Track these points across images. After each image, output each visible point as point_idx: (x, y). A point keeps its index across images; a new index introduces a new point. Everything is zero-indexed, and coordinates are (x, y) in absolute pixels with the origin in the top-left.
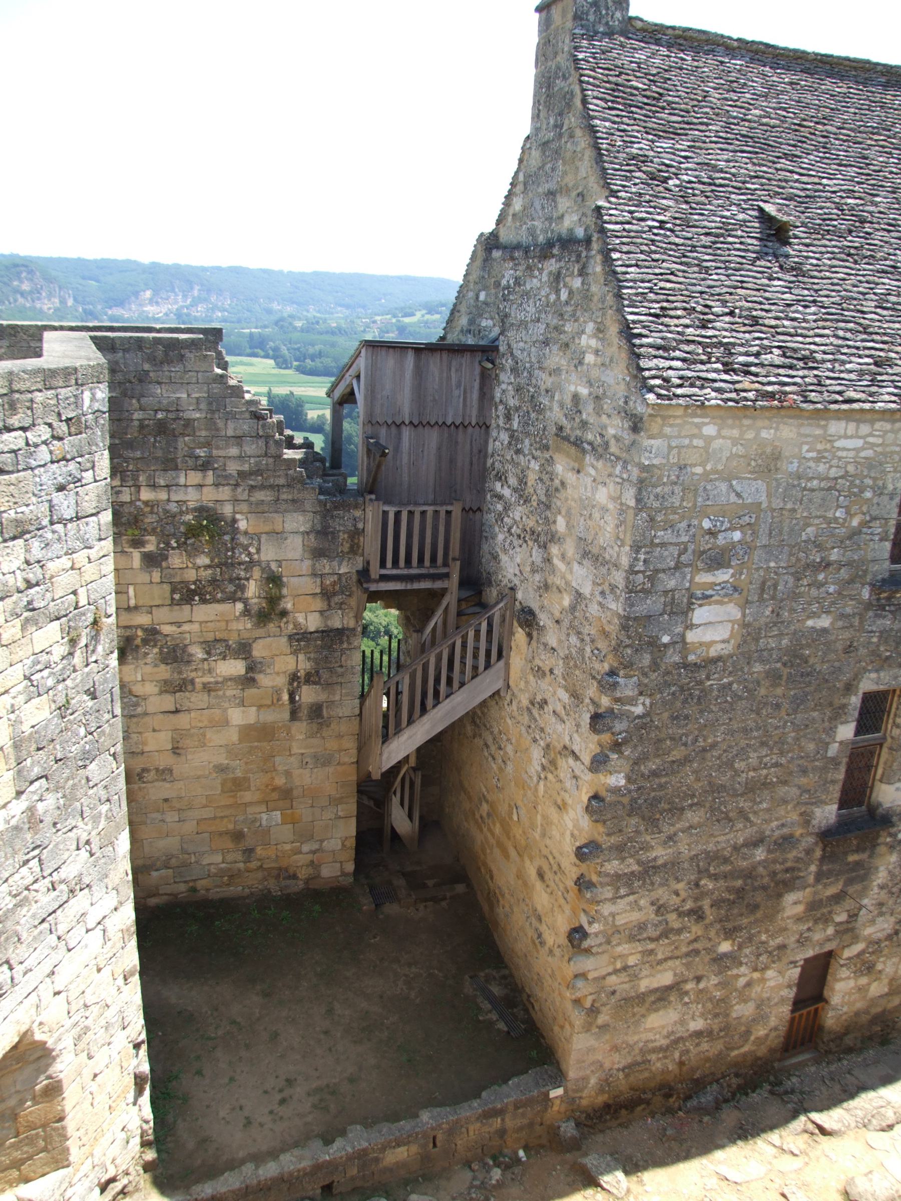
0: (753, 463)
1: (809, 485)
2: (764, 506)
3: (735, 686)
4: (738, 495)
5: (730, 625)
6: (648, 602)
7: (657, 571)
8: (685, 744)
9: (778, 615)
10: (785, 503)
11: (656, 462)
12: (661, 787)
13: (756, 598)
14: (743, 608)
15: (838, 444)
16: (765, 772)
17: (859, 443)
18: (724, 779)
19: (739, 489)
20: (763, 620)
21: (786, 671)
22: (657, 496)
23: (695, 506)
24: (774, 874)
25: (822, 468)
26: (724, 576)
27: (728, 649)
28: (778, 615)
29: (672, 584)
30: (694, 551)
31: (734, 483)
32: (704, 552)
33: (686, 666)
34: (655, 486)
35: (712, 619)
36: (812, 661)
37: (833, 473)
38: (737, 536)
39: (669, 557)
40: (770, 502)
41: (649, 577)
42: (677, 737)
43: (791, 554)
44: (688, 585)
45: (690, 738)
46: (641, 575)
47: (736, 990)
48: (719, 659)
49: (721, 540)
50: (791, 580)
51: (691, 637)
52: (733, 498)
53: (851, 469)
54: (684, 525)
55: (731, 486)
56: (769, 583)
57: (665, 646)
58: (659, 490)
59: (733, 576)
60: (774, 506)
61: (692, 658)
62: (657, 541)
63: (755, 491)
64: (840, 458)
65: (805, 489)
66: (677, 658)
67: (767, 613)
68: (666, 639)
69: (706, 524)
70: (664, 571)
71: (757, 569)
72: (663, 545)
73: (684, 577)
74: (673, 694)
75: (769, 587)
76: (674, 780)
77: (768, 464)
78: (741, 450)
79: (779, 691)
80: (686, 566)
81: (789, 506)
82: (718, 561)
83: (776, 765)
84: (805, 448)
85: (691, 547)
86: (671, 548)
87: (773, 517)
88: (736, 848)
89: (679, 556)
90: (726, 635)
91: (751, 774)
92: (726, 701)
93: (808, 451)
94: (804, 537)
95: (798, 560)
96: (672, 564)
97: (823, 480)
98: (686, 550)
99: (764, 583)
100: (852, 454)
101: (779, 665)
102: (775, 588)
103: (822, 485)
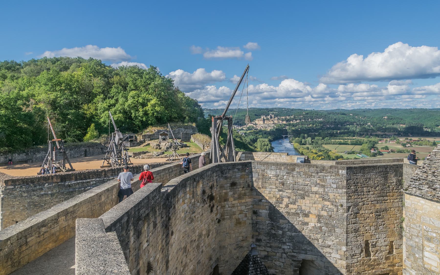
22: (410, 214)
23: (421, 220)
26: (433, 246)
29: (417, 240)
30: (422, 234)
32: (425, 235)
33: (425, 268)
35: (430, 257)
38: (434, 235)
39: (415, 232)
51: (425, 259)
54: (418, 225)
61: (426, 266)
72: (413, 228)
73: (420, 240)
78: (432, 210)
85: (421, 232)
90: (436, 265)
96: (416, 235)
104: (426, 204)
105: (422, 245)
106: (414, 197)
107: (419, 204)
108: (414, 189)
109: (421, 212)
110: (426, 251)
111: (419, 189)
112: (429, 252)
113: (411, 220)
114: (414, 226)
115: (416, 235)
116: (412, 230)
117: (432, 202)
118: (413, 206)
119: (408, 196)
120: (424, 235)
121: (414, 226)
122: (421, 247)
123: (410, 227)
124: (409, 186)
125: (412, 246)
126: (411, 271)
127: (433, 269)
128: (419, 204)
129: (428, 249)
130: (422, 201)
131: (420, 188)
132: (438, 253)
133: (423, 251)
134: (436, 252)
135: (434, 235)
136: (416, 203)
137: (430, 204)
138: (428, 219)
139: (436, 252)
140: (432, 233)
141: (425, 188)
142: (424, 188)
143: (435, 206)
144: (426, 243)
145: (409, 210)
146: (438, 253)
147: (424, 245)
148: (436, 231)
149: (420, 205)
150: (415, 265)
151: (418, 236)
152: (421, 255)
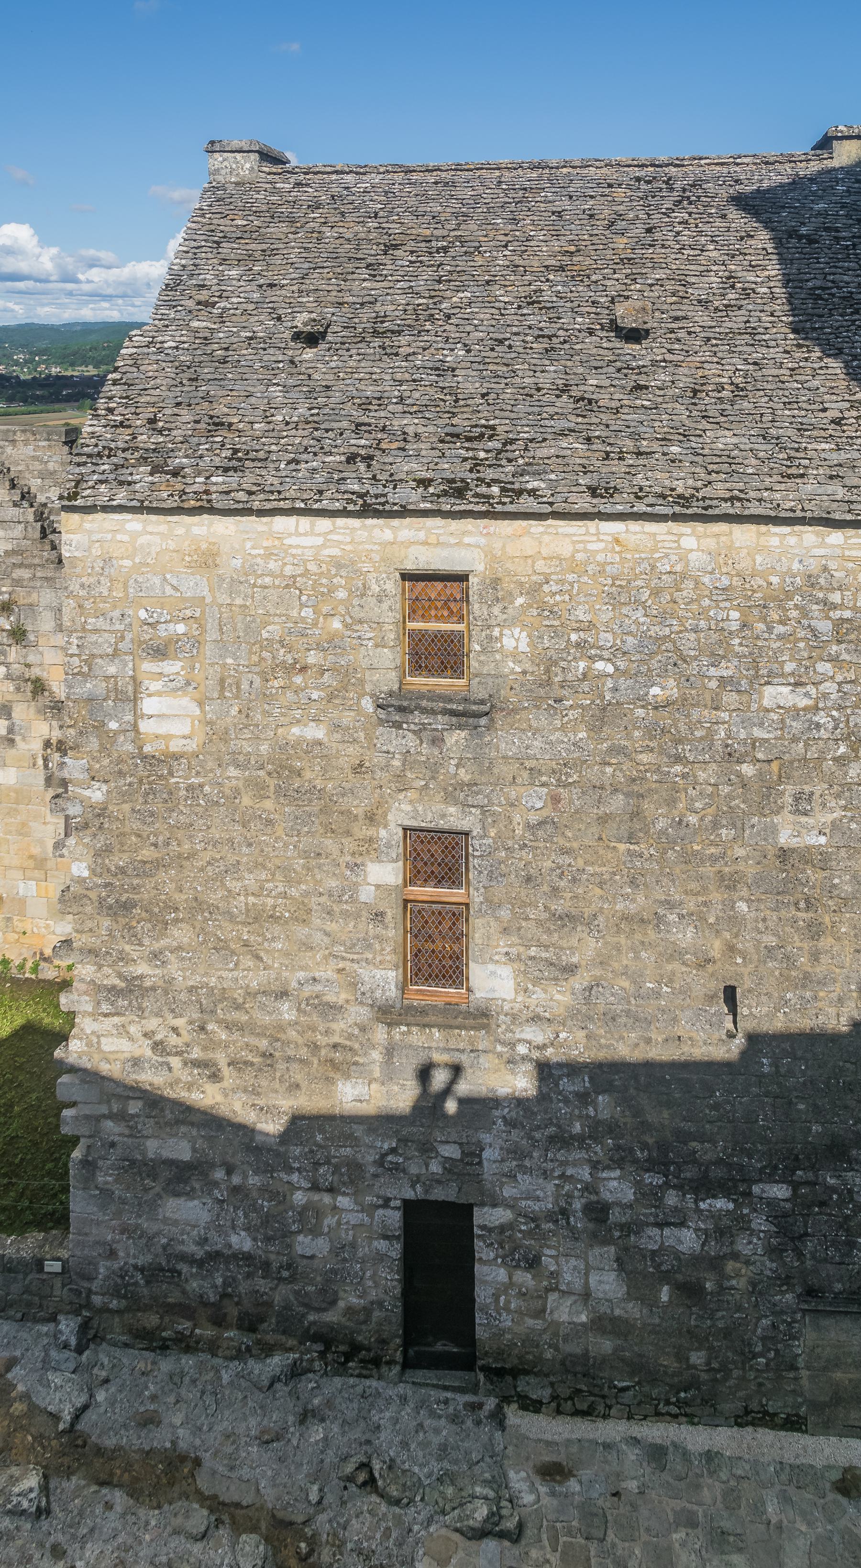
0: (187, 558)
1: (259, 581)
2: (208, 600)
3: (207, 789)
4: (175, 588)
5: (189, 721)
6: (88, 685)
7: (93, 656)
8: (155, 845)
9: (247, 716)
10: (233, 599)
11: (76, 554)
12: (135, 889)
13: (216, 695)
14: (201, 704)
15: (287, 542)
16: (270, 901)
17: (320, 541)
18: (215, 897)
19: (174, 582)
20: (229, 720)
21: (272, 783)
22: (82, 586)
25: (272, 565)
26: (172, 667)
27: (192, 746)
28: (247, 716)
29: (112, 670)
30: (132, 641)
31: (168, 576)
32: (145, 642)
33: (144, 757)
34: (79, 576)
35: (165, 711)
36: (308, 775)
37: (288, 570)
38: (181, 628)
39: (105, 643)
40: (214, 597)
41: (86, 661)
42: (145, 835)
43: (251, 653)
44: (131, 673)
45: (161, 838)
46: (76, 659)
49: (163, 631)
50: (257, 681)
51: (144, 726)
52: (169, 591)
53: (312, 567)
54: (116, 614)
55: (165, 579)
56: (229, 681)
57: (116, 733)
58: (84, 579)
59: (183, 668)
60: (220, 601)
61: (147, 749)
62: (89, 627)
63: (194, 585)
64: (294, 556)
65: (254, 585)
66: (130, 748)
67: (234, 711)
68: (113, 725)
69: (143, 614)
70: (101, 657)
71: (212, 665)
73: (126, 665)
74: (130, 785)
75: (230, 685)
76: (149, 883)
77: (206, 560)
79: (269, 804)
80: (126, 653)
81: (239, 601)
83: (284, 895)
84: (249, 545)
85: (129, 636)
86: (106, 635)
87: (221, 613)
88: (250, 994)
89: (116, 644)
90: (187, 731)
91: (251, 899)
92: (199, 805)
93: (253, 548)
94: (265, 635)
95: (262, 659)
96: (110, 651)
97: (276, 577)
98: (123, 638)
99: (222, 681)
100: (309, 553)
101: (261, 773)
102: (238, 688)
103: (277, 582)
104: (150, 529)
105: (134, 678)
106: (100, 516)
107: (119, 537)
108: (103, 488)
109: (127, 563)
110: (149, 695)
111: (121, 483)
112: (159, 694)
113: (88, 605)
114: (101, 623)
115: (110, 651)
116: (94, 638)
117: (169, 518)
118: (96, 551)
119: (76, 517)
120: (141, 643)
121: (101, 623)
122: (130, 688)
123: (84, 630)
124: (78, 483)
125: (90, 700)
126: (87, 793)
127: (175, 746)
128: (119, 537)
129: (155, 686)
130: (133, 523)
131: (122, 478)
132: (194, 685)
133: (135, 700)
134: (188, 683)
135: (181, 628)
136: (109, 536)
137: (163, 528)
138: (157, 580)
139: (188, 683)
140: (171, 625)
141: (142, 475)
142: (136, 477)
143: (180, 531)
144: (148, 666)
145: (78, 570)
146: (194, 685)
147: (140, 678)
148: (188, 613)
149: (125, 538)
150: (106, 762)
151: (116, 654)
152: (129, 717)
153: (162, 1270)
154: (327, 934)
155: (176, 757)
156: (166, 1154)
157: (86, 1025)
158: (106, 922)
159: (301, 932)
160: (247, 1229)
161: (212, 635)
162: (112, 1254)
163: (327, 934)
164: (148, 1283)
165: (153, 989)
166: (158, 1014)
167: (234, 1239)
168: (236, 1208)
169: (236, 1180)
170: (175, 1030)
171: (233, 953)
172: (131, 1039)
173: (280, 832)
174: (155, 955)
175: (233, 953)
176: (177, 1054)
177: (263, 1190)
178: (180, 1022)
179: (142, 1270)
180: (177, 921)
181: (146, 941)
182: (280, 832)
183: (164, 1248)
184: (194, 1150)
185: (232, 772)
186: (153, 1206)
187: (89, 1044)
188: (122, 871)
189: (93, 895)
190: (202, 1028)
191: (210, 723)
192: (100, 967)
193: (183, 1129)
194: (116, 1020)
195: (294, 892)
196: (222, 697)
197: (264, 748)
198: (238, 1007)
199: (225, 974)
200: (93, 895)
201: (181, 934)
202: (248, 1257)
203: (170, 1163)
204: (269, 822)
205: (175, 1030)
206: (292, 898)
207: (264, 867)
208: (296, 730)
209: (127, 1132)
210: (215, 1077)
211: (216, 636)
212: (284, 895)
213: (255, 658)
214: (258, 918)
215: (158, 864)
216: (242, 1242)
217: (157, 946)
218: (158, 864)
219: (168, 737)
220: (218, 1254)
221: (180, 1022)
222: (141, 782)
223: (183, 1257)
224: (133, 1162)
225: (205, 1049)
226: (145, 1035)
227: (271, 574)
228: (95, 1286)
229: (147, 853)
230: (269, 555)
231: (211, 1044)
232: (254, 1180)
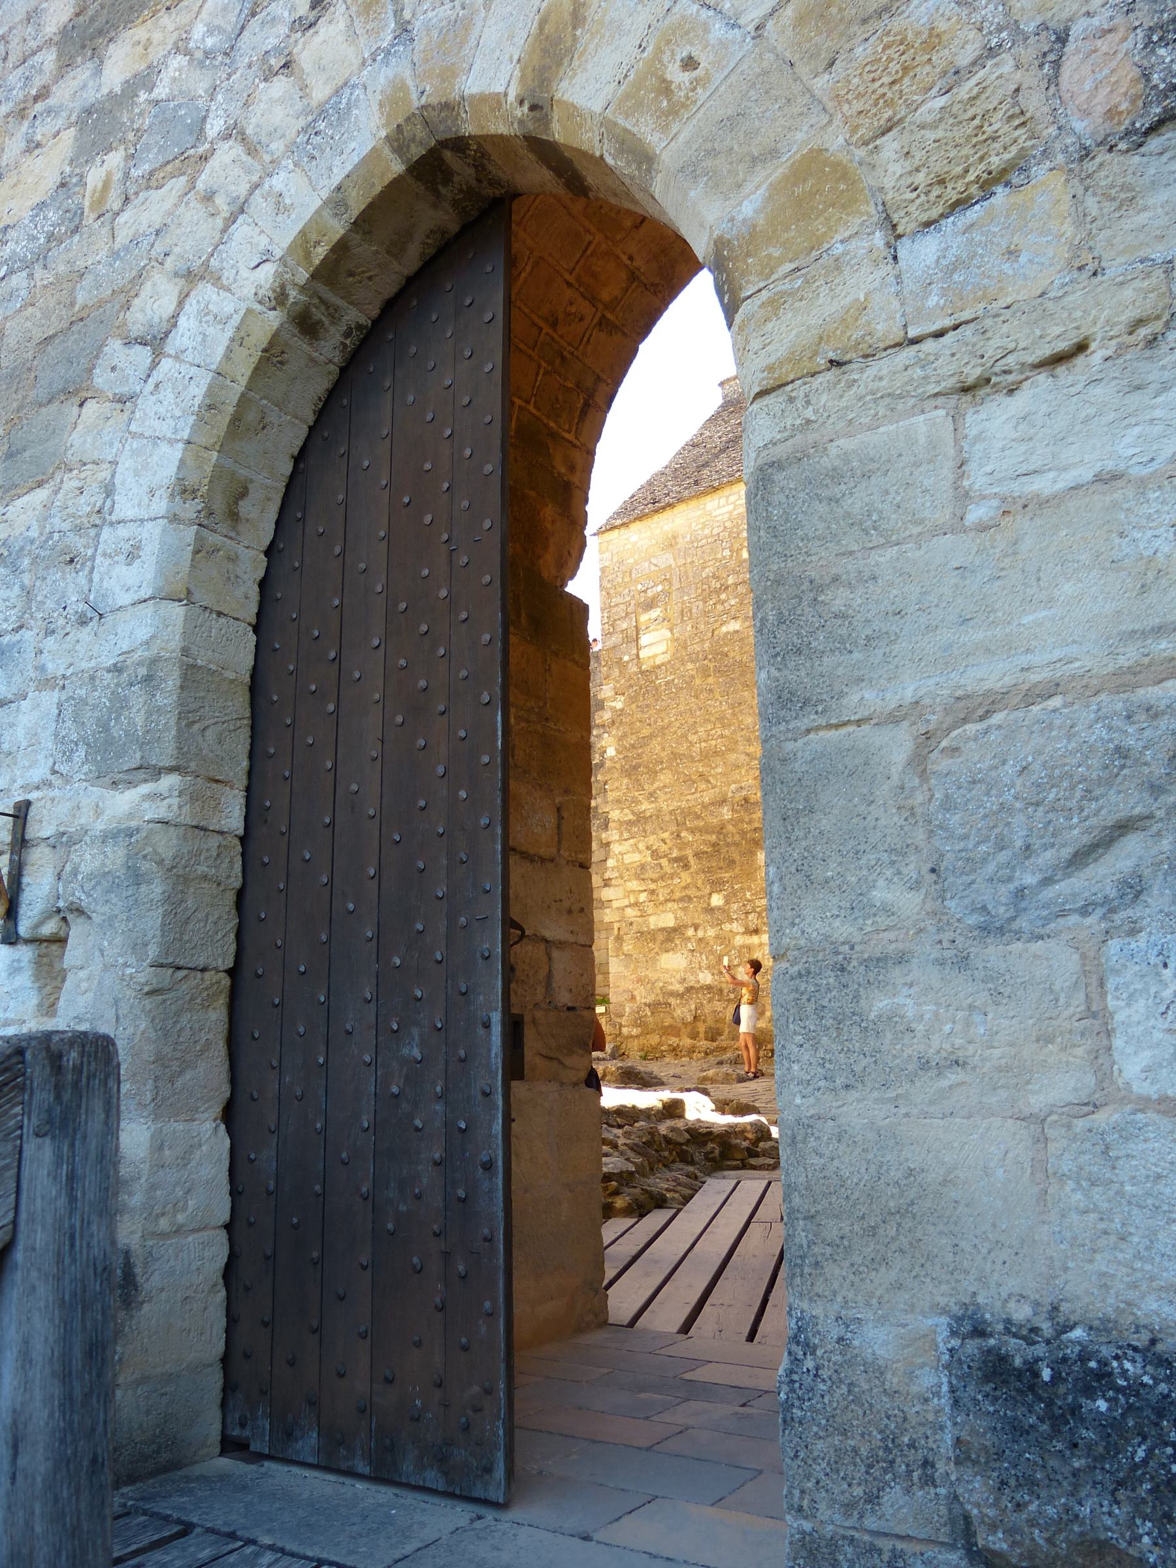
12: (639, 756)
14: (671, 630)
16: (713, 742)
17: (731, 507)
18: (682, 749)
20: (687, 634)
21: (712, 665)
24: (743, 833)
25: (707, 532)
26: (655, 613)
27: (667, 657)
29: (625, 625)
33: (642, 672)
36: (732, 654)
37: (715, 532)
47: (734, 948)
48: (663, 664)
49: (650, 594)
50: (701, 603)
52: (653, 568)
53: (728, 524)
54: (626, 591)
57: (627, 662)
61: (644, 667)
63: (666, 559)
66: (635, 669)
67: (689, 628)
68: (626, 658)
69: (639, 587)
76: (647, 749)
79: (711, 680)
81: (689, 560)
82: (650, 605)
83: (722, 736)
85: (633, 602)
88: (704, 807)
91: (703, 744)
95: (704, 590)
100: (727, 516)
113: (612, 591)
138: (646, 564)
153: (660, 1004)
154: (747, 754)
155: (659, 667)
156: (661, 925)
157: (616, 848)
158: (625, 781)
159: (732, 757)
160: (708, 968)
161: (676, 585)
162: (633, 998)
163: (747, 754)
164: (652, 1013)
165: (651, 817)
166: (654, 833)
167: (701, 976)
168: (701, 954)
169: (700, 934)
170: (663, 841)
171: (694, 782)
172: (640, 852)
173: (717, 696)
174: (651, 795)
175: (694, 782)
176: (666, 856)
177: (717, 937)
178: (666, 835)
179: (649, 1006)
180: (662, 769)
181: (646, 787)
182: (717, 696)
183: (661, 989)
184: (676, 918)
185: (690, 666)
186: (654, 961)
187: (617, 861)
188: (633, 746)
189: (618, 766)
190: (678, 836)
191: (677, 639)
192: (622, 809)
193: (669, 905)
194: (632, 841)
195: (727, 732)
196: (683, 621)
197: (707, 645)
198: (698, 817)
199: (689, 797)
200: (618, 766)
201: (665, 778)
202: (709, 988)
203: (663, 929)
204: (711, 690)
205: (663, 841)
206: (726, 737)
207: (709, 721)
208: (724, 629)
209: (639, 914)
210: (686, 866)
211: (678, 586)
212: (722, 736)
213: (699, 591)
214: (707, 756)
215: (652, 736)
216: (706, 978)
217: (652, 789)
218: (652, 736)
219: (656, 656)
220: (692, 988)
221: (666, 835)
222: (641, 688)
223: (672, 994)
224: (642, 933)
225: (680, 849)
226: (647, 848)
227: (706, 537)
228: (624, 1021)
229: (646, 732)
230: (705, 526)
231: (683, 845)
232: (711, 933)
